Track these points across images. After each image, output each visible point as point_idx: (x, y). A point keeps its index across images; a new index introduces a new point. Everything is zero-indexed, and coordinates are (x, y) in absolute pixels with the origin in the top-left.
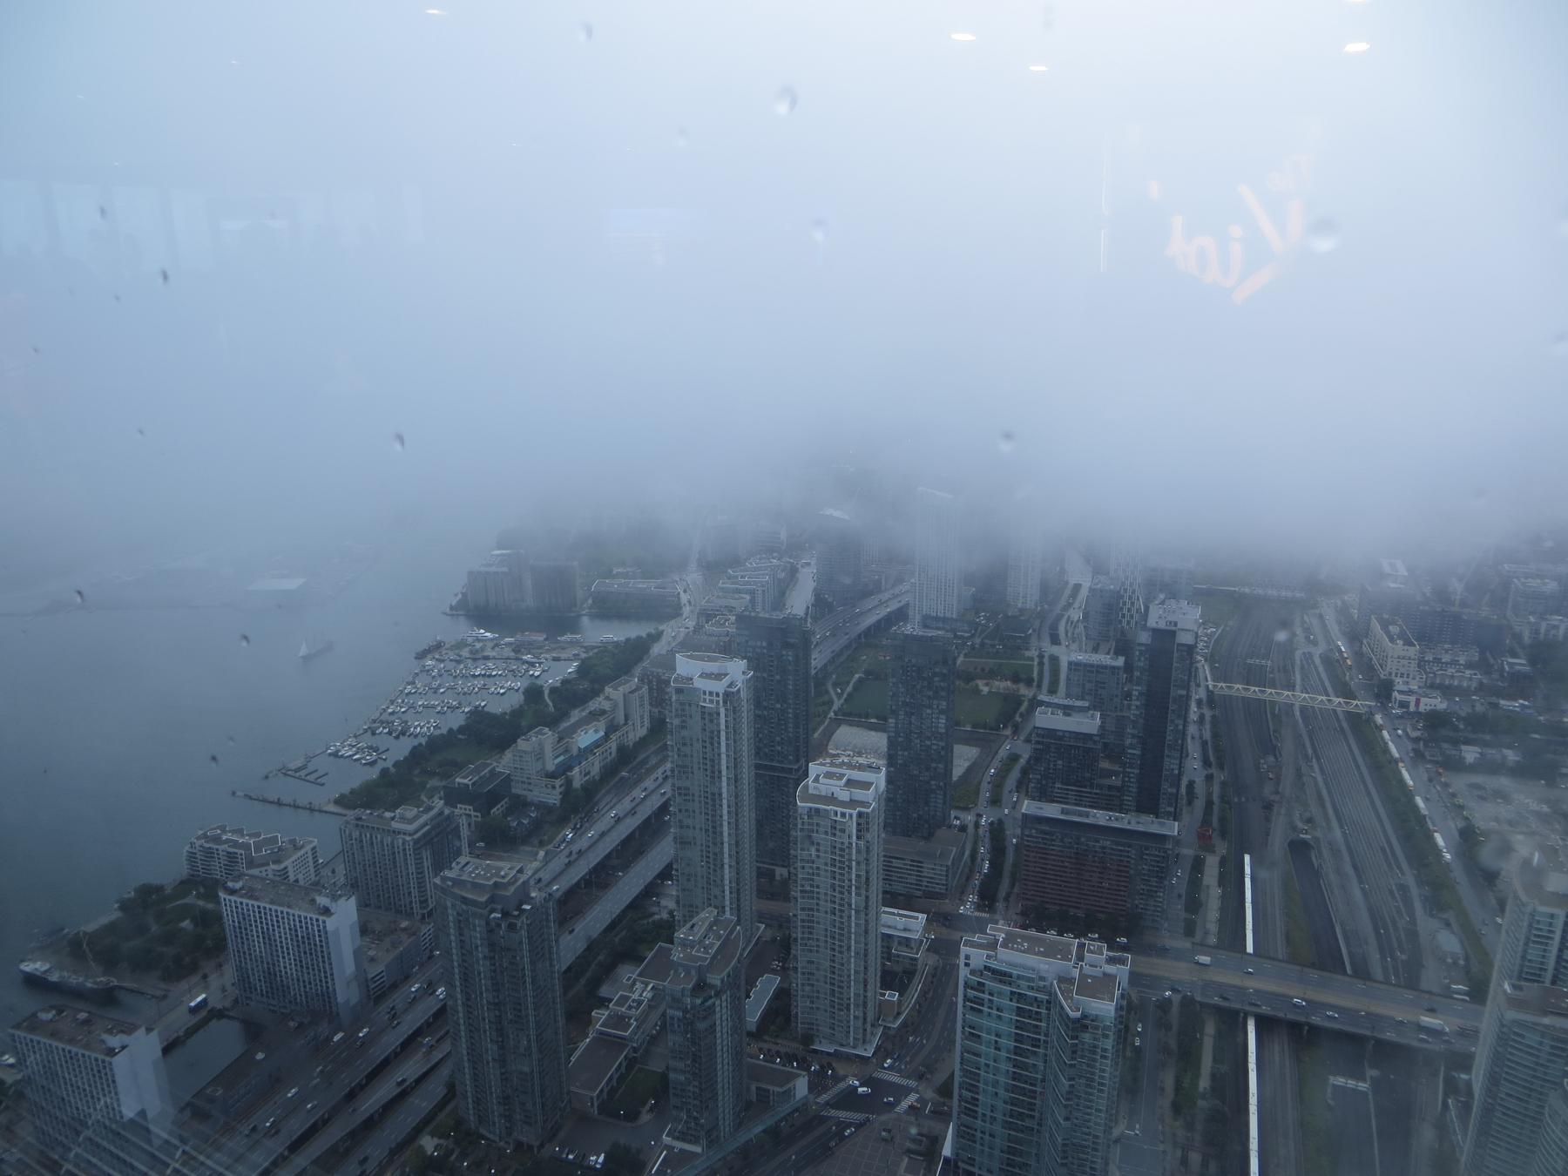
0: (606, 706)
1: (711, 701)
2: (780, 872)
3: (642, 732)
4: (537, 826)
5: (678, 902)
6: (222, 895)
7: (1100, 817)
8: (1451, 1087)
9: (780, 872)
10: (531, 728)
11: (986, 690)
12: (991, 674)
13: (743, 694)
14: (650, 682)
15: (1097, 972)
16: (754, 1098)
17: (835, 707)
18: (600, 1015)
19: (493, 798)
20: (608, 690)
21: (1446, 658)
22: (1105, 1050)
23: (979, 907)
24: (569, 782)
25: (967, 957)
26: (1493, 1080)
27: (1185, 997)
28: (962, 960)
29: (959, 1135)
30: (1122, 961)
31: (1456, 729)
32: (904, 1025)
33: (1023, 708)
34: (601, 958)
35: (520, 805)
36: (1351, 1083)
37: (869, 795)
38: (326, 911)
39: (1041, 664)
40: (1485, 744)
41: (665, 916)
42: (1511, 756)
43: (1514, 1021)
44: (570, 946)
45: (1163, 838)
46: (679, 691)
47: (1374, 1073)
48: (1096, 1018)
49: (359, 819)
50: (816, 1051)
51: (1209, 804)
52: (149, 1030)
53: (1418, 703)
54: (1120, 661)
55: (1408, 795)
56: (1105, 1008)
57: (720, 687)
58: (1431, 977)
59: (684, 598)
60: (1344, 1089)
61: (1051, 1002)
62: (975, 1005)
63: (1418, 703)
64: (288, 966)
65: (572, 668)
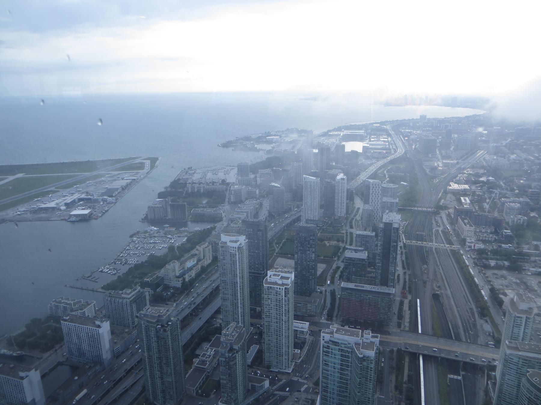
0: (197, 252)
1: (233, 250)
2: (258, 309)
3: (209, 261)
4: (173, 295)
5: (223, 320)
7: (368, 287)
8: (489, 377)
9: (258, 309)
10: (170, 261)
11: (328, 244)
12: (329, 239)
14: (212, 244)
15: (368, 341)
16: (250, 388)
17: (277, 251)
18: (196, 361)
19: (158, 285)
20: (197, 247)
21: (484, 231)
22: (371, 368)
23: (327, 320)
24: (184, 279)
25: (323, 337)
26: (503, 375)
27: (398, 349)
28: (322, 338)
29: (322, 399)
30: (377, 337)
31: (487, 255)
32: (302, 361)
33: (341, 251)
34: (196, 340)
36: (456, 377)
37: (289, 282)
38: (99, 327)
39: (347, 235)
40: (497, 259)
41: (218, 325)
42: (507, 263)
43: (510, 354)
44: (185, 336)
45: (389, 294)
46: (222, 247)
47: (463, 373)
48: (368, 357)
49: (110, 294)
50: (271, 371)
51: (405, 282)
52: (36, 370)
53: (474, 246)
54: (374, 234)
55: (472, 277)
56: (371, 353)
57: (236, 245)
58: (481, 339)
59: (223, 215)
60: (453, 379)
61: (353, 352)
62: (326, 353)
63: (474, 246)
64: (85, 346)
65: (185, 239)
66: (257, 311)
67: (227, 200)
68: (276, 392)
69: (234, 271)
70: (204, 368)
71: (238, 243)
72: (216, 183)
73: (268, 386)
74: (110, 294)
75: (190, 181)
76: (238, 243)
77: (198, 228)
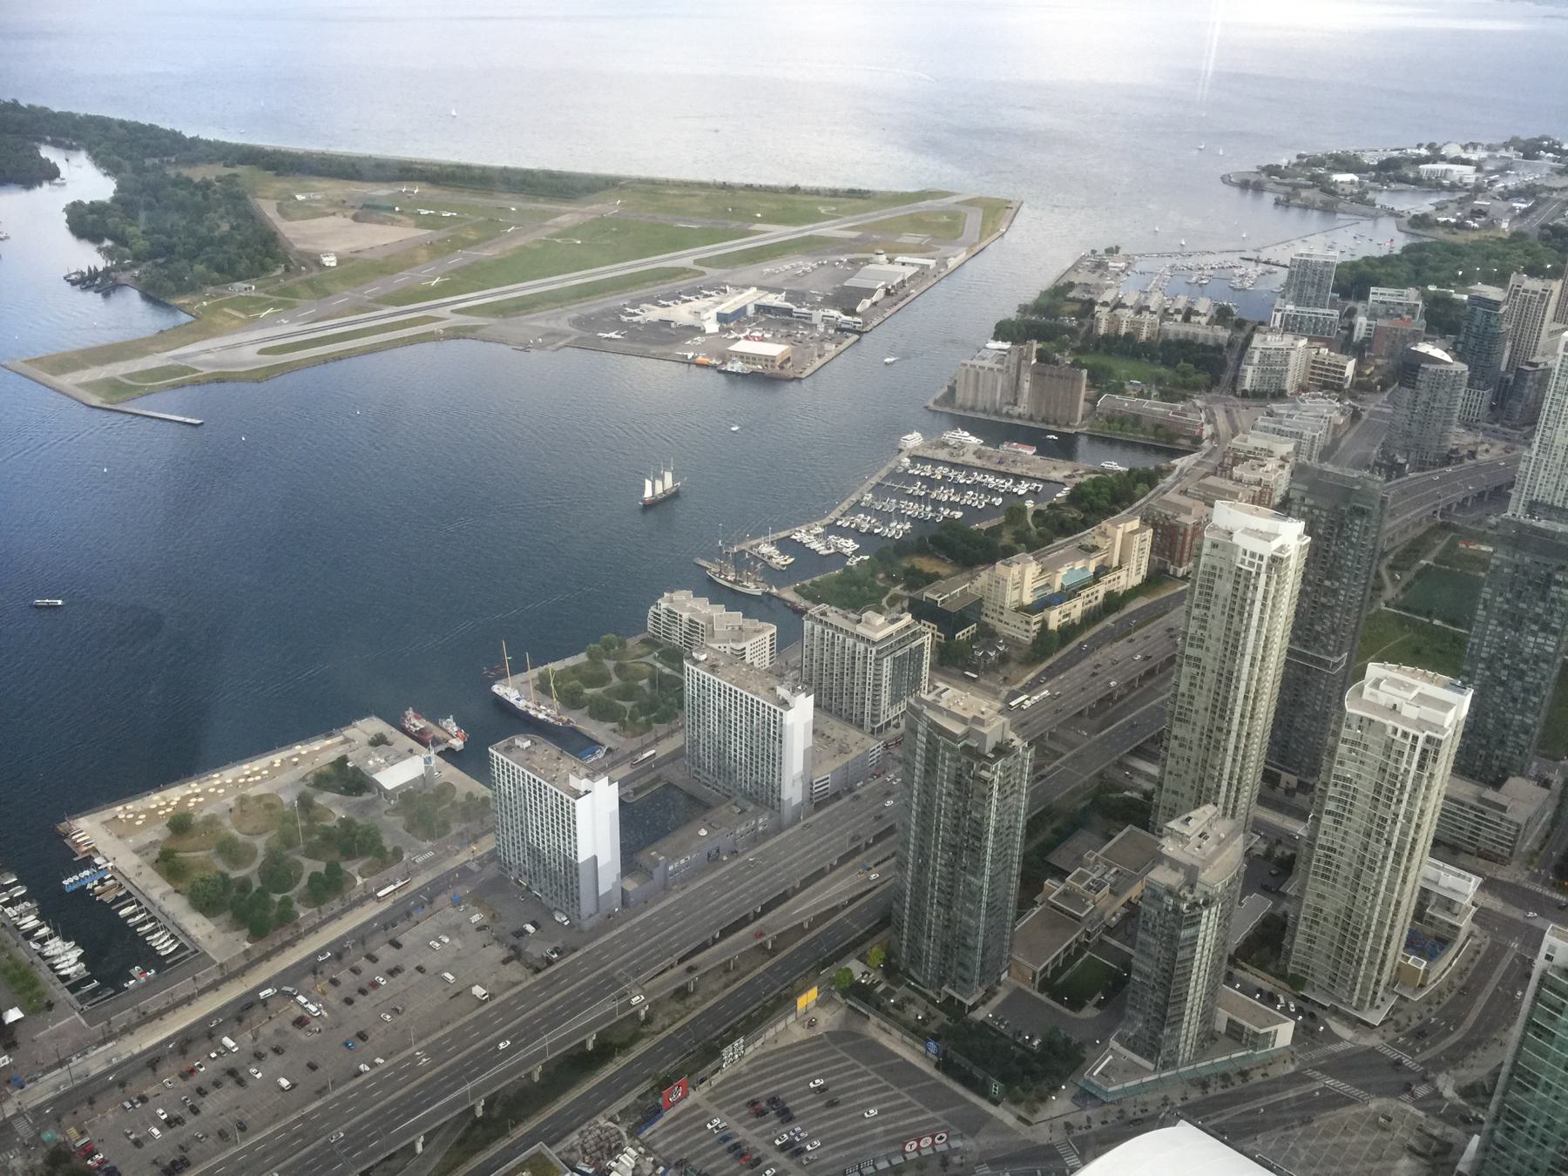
2: (1288, 779)
3: (1136, 580)
4: (1004, 659)
6: (686, 664)
9: (1288, 779)
13: (1293, 563)
16: (1221, 1026)
17: (1390, 592)
20: (1104, 524)
24: (1044, 623)
35: (987, 635)
38: (785, 704)
41: (1135, 795)
49: (824, 614)
52: (611, 782)
57: (1268, 549)
59: (1208, 430)
64: (738, 749)
66: (1283, 784)
67: (1227, 377)
68: (1309, 1073)
69: (1238, 634)
70: (1078, 919)
71: (1275, 544)
72: (1197, 314)
73: (1288, 1041)
74: (824, 614)
75: (1108, 296)
76: (1275, 544)
77: (1114, 466)
